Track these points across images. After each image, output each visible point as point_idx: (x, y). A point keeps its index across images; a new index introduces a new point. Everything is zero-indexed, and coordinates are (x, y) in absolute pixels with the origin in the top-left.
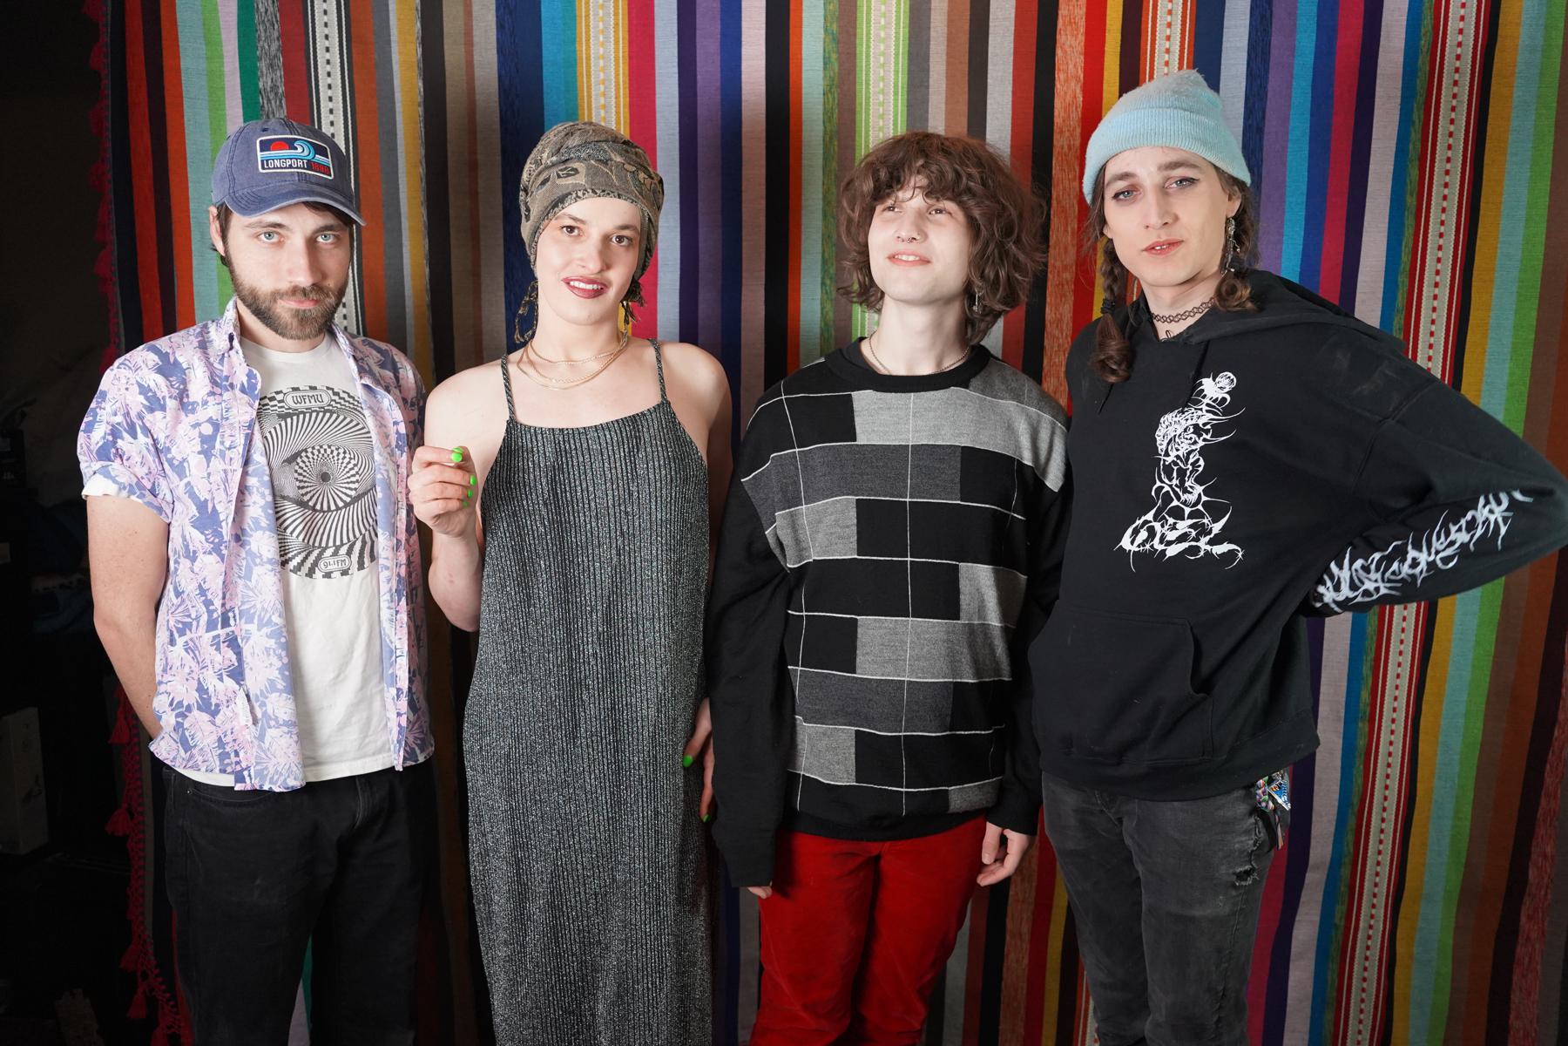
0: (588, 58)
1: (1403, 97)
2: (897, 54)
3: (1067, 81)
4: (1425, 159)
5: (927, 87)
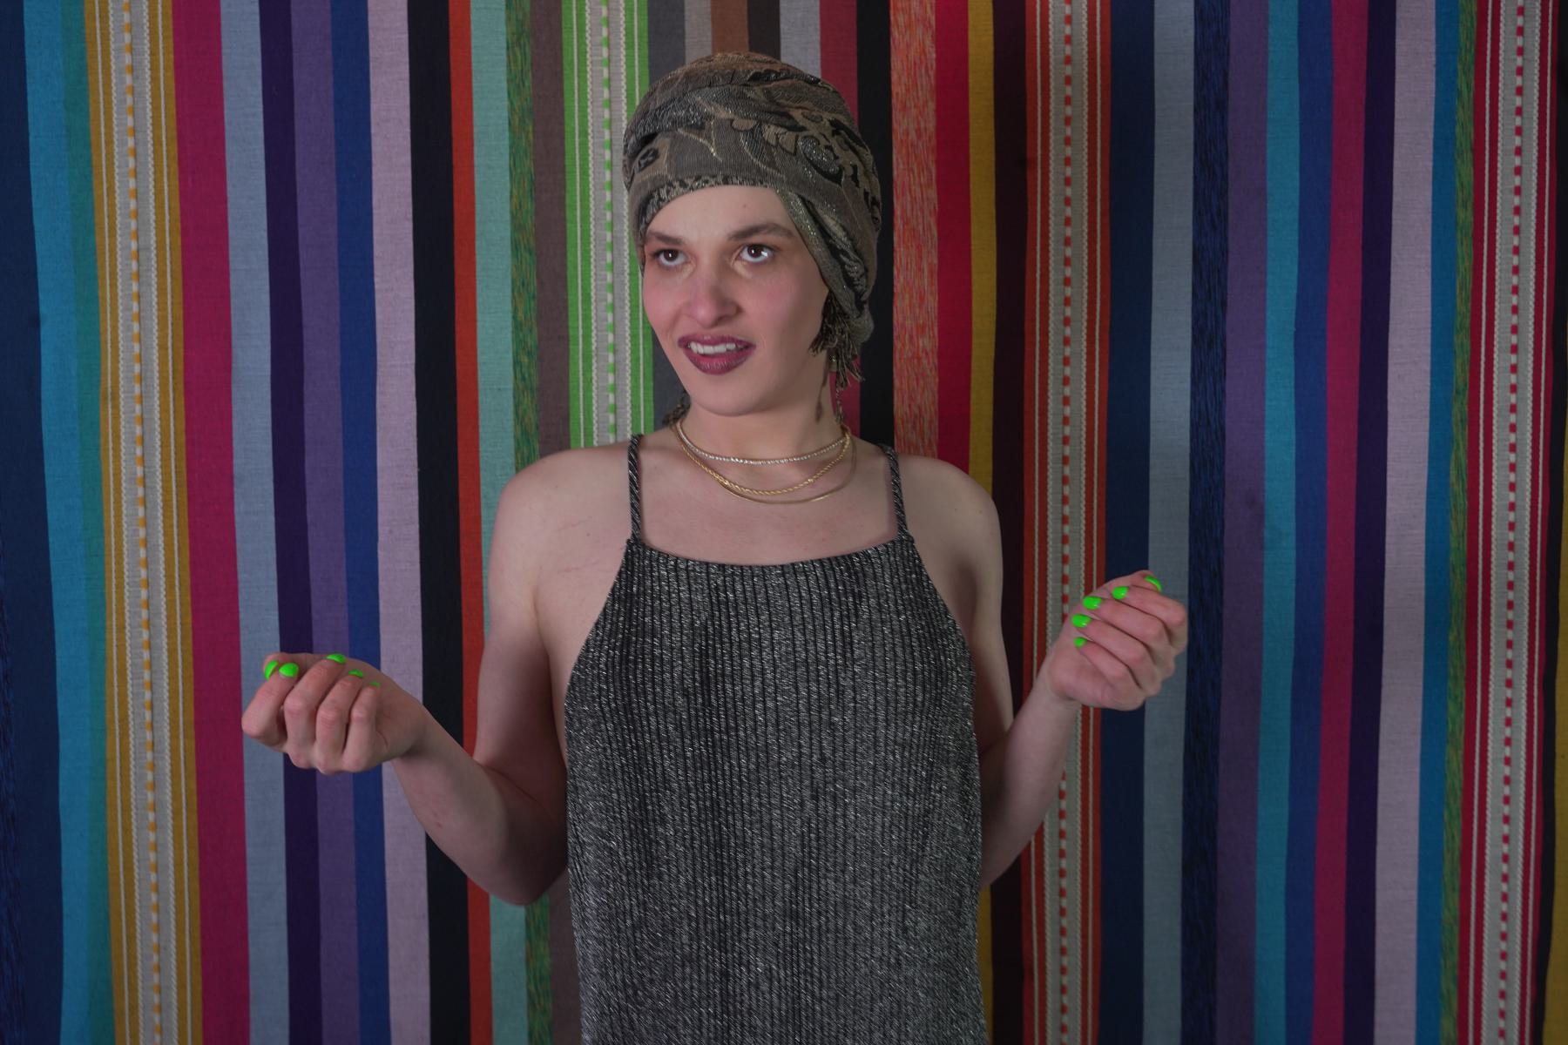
1: (1439, 53)
3: (908, 26)
4: (1482, 150)
5: (682, 37)
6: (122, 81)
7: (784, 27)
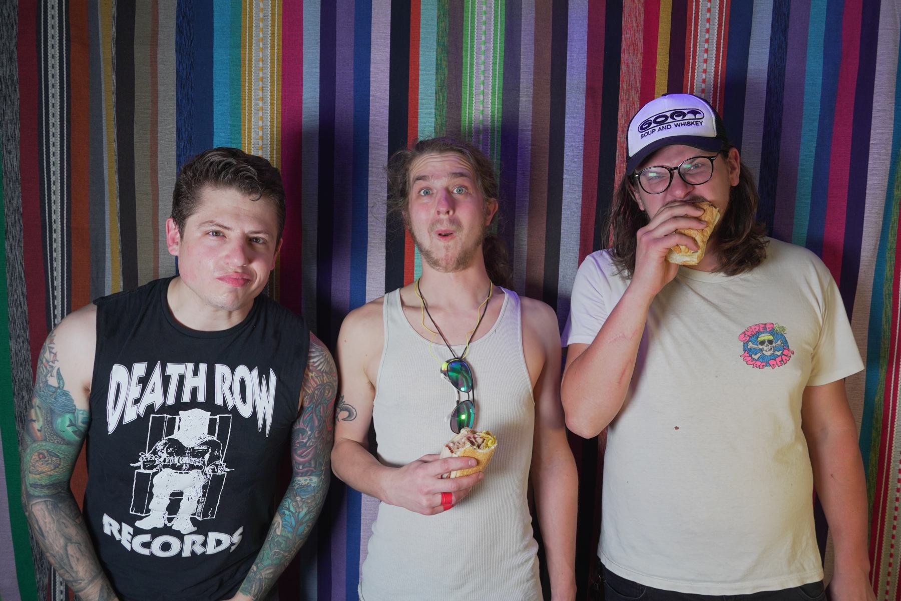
0: (250, 60)
2: (494, 64)
3: (629, 90)
6: (257, 104)
7: (567, 88)
